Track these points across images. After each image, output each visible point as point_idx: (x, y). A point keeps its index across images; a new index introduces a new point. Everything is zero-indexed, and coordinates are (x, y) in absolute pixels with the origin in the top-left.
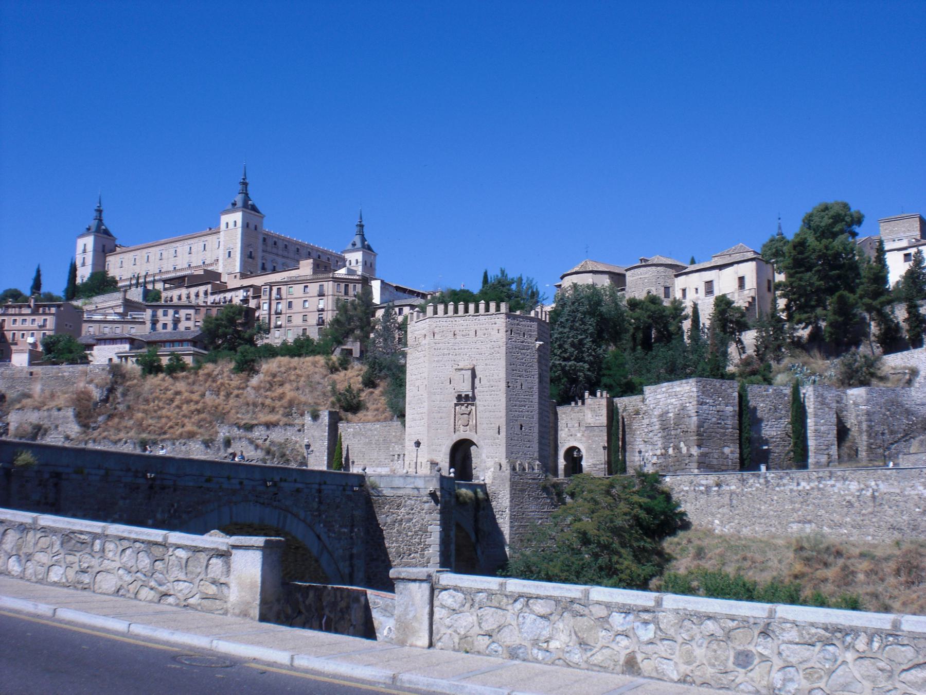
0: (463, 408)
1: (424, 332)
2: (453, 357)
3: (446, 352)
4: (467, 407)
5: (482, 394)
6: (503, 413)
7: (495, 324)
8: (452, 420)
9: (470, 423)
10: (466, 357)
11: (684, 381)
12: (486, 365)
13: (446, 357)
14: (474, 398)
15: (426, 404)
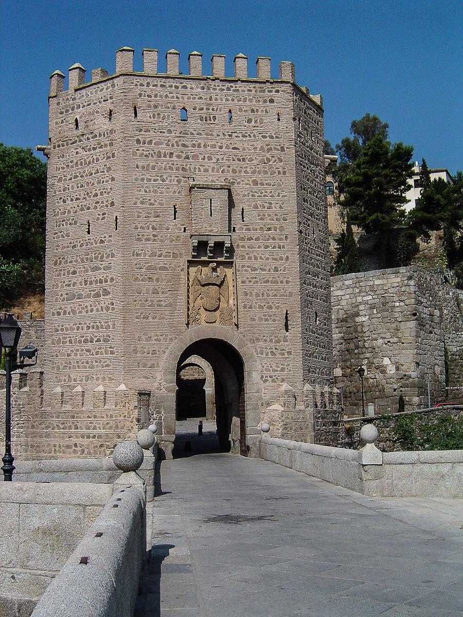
0: (206, 270)
1: (108, 106)
2: (181, 162)
3: (163, 148)
4: (214, 270)
5: (247, 243)
6: (294, 286)
7: (272, 101)
8: (183, 298)
9: (223, 305)
10: (210, 164)
11: (389, 270)
12: (255, 183)
13: (164, 162)
14: (231, 251)
15: (117, 260)
